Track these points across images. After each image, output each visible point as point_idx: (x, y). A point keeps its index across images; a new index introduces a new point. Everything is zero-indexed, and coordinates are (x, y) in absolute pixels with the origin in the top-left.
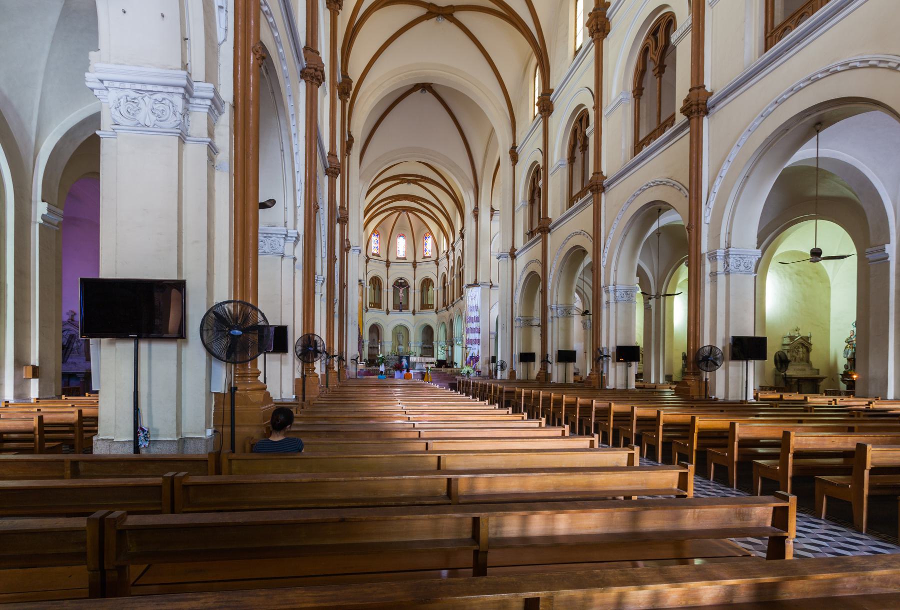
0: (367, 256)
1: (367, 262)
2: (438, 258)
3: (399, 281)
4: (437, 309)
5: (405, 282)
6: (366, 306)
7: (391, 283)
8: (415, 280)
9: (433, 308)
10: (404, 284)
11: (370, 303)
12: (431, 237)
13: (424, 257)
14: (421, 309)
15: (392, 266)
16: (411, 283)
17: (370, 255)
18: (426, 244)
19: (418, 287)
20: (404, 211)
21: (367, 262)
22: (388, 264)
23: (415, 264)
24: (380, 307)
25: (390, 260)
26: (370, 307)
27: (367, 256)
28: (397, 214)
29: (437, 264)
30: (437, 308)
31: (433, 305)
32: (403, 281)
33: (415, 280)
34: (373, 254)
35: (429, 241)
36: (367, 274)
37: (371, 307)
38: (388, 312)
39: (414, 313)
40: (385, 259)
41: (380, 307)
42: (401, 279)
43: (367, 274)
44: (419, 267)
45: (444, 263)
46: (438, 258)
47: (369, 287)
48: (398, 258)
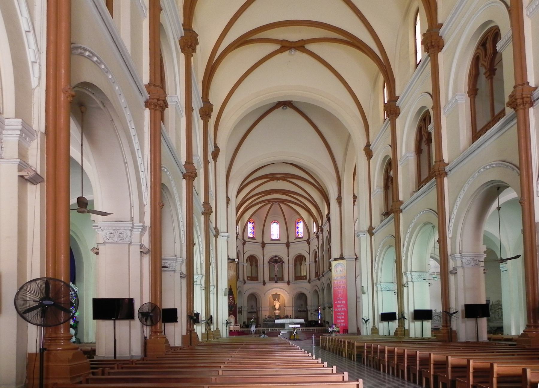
0: (243, 239)
1: (244, 244)
2: (309, 238)
3: (274, 258)
4: (310, 279)
5: (280, 258)
6: (244, 279)
7: (267, 259)
8: (288, 257)
9: (306, 279)
10: (279, 260)
11: (247, 277)
12: (302, 221)
13: (297, 238)
14: (295, 279)
15: (267, 247)
16: (285, 259)
17: (246, 239)
18: (298, 228)
19: (292, 262)
20: (276, 202)
21: (244, 244)
22: (263, 245)
23: (288, 244)
24: (257, 280)
25: (265, 241)
26: (247, 280)
27: (243, 239)
28: (270, 205)
29: (309, 243)
30: (310, 278)
31: (306, 276)
32: (278, 258)
33: (288, 257)
34: (250, 238)
35: (301, 225)
36: (244, 254)
37: (249, 280)
38: (264, 283)
39: (288, 283)
40: (261, 241)
41: (257, 280)
42: (276, 256)
43: (244, 254)
44: (291, 246)
45: (314, 242)
46: (309, 238)
47: (246, 264)
48: (272, 240)
